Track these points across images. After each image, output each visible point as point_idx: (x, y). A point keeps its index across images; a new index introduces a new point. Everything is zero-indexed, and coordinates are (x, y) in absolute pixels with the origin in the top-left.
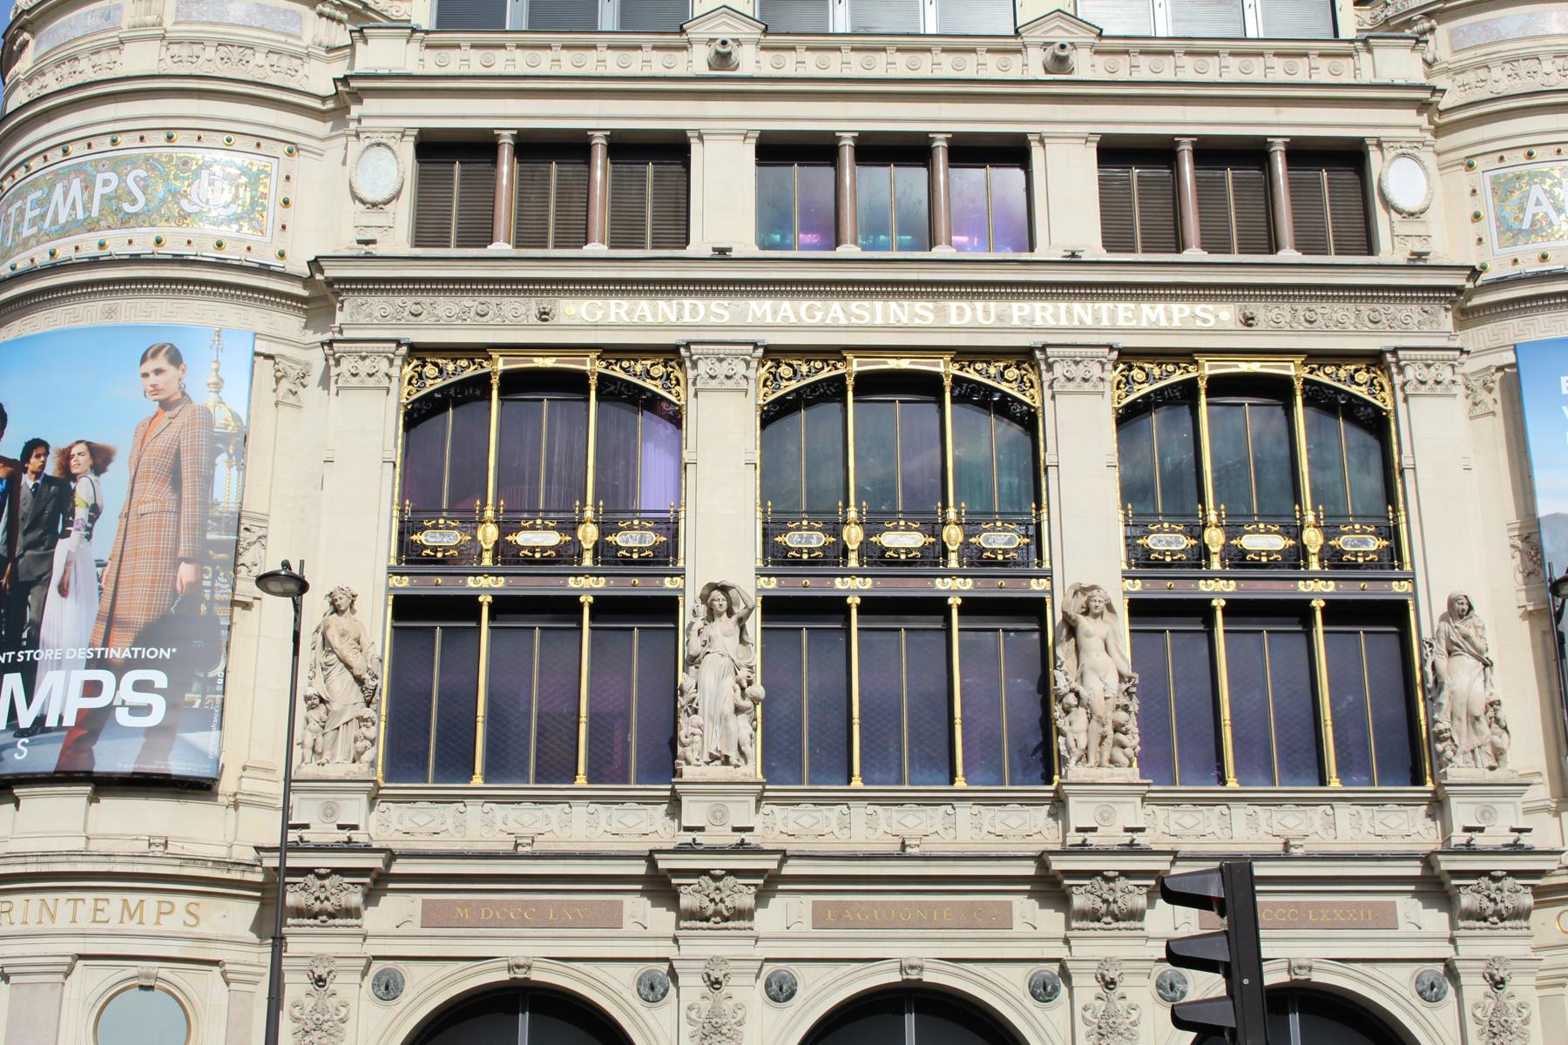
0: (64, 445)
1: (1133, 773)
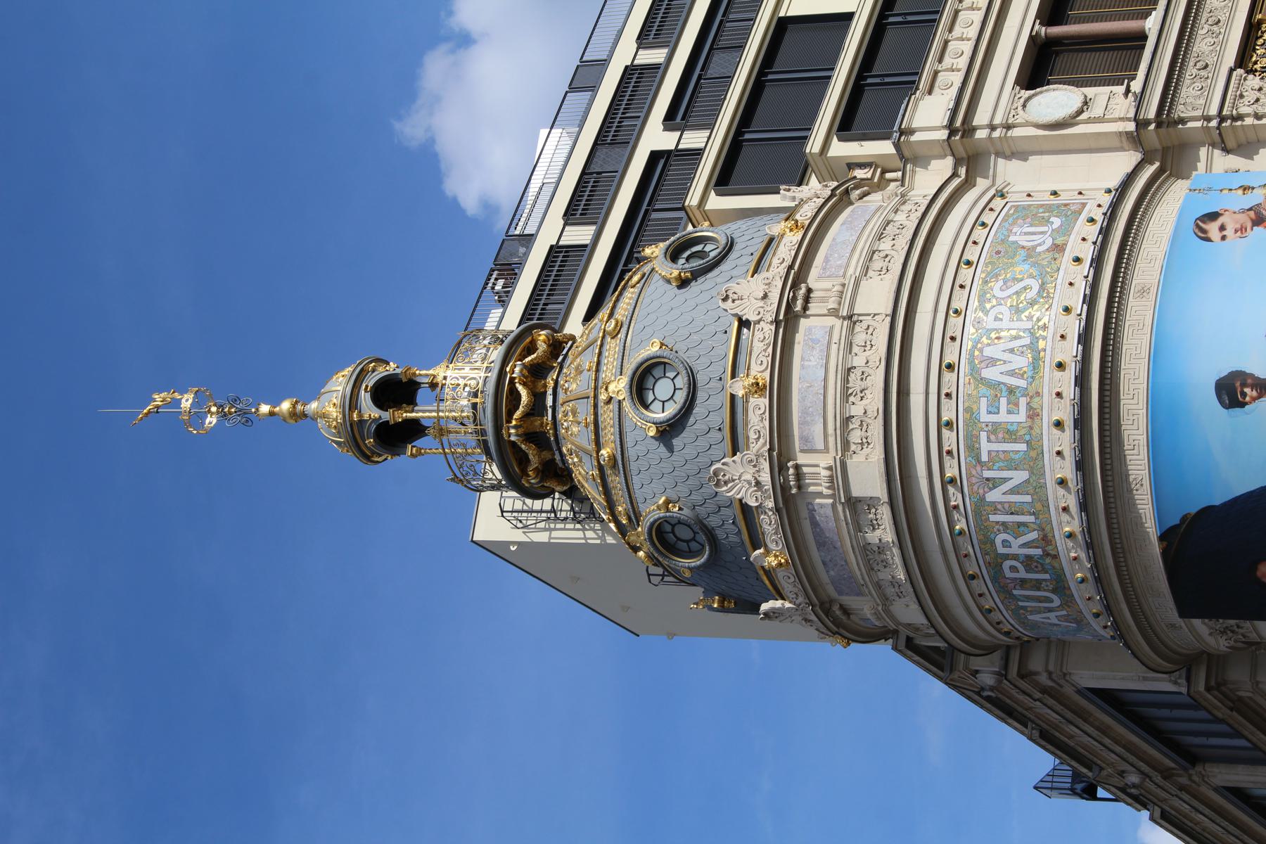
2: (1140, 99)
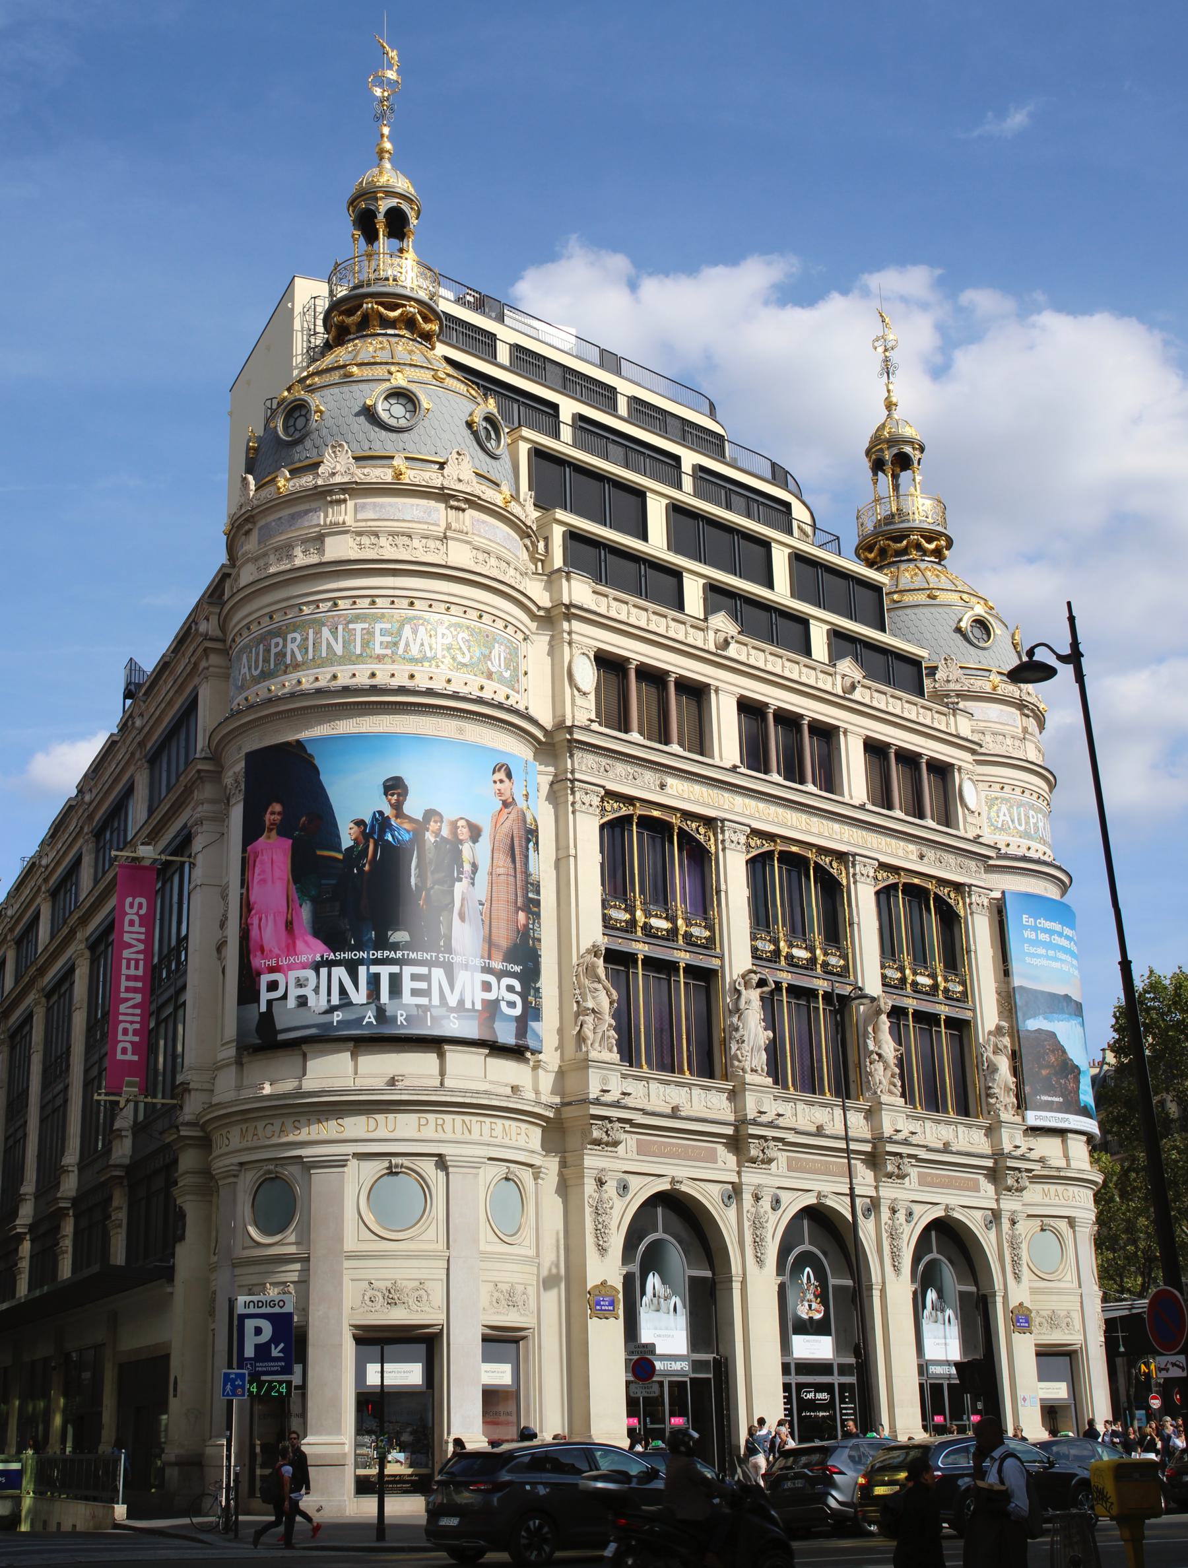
0: (454, 818)
1: (615, 1057)
2: (586, 729)
